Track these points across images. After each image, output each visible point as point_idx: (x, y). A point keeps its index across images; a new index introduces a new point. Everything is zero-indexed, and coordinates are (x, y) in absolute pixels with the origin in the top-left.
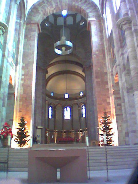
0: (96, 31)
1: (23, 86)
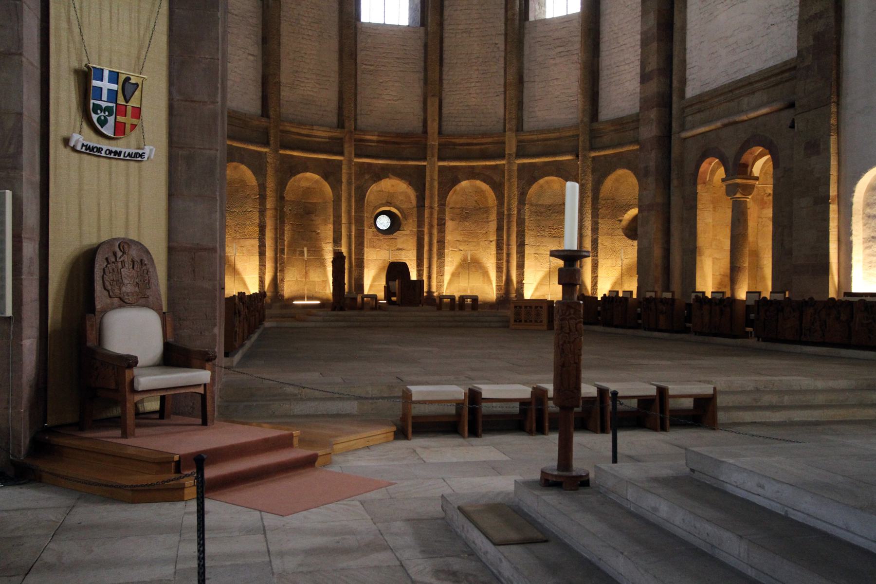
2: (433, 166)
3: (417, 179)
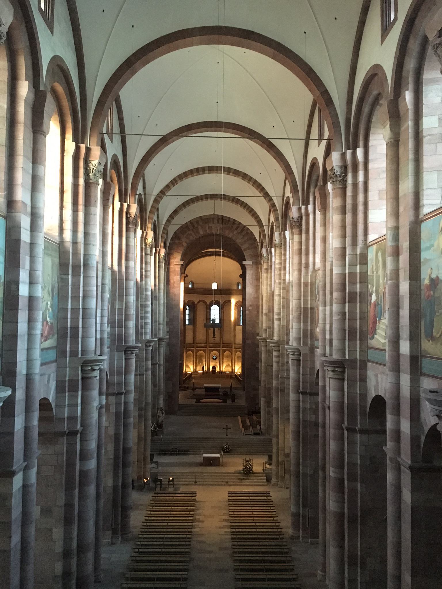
1: (168, 345)
2: (222, 349)
3: (219, 351)
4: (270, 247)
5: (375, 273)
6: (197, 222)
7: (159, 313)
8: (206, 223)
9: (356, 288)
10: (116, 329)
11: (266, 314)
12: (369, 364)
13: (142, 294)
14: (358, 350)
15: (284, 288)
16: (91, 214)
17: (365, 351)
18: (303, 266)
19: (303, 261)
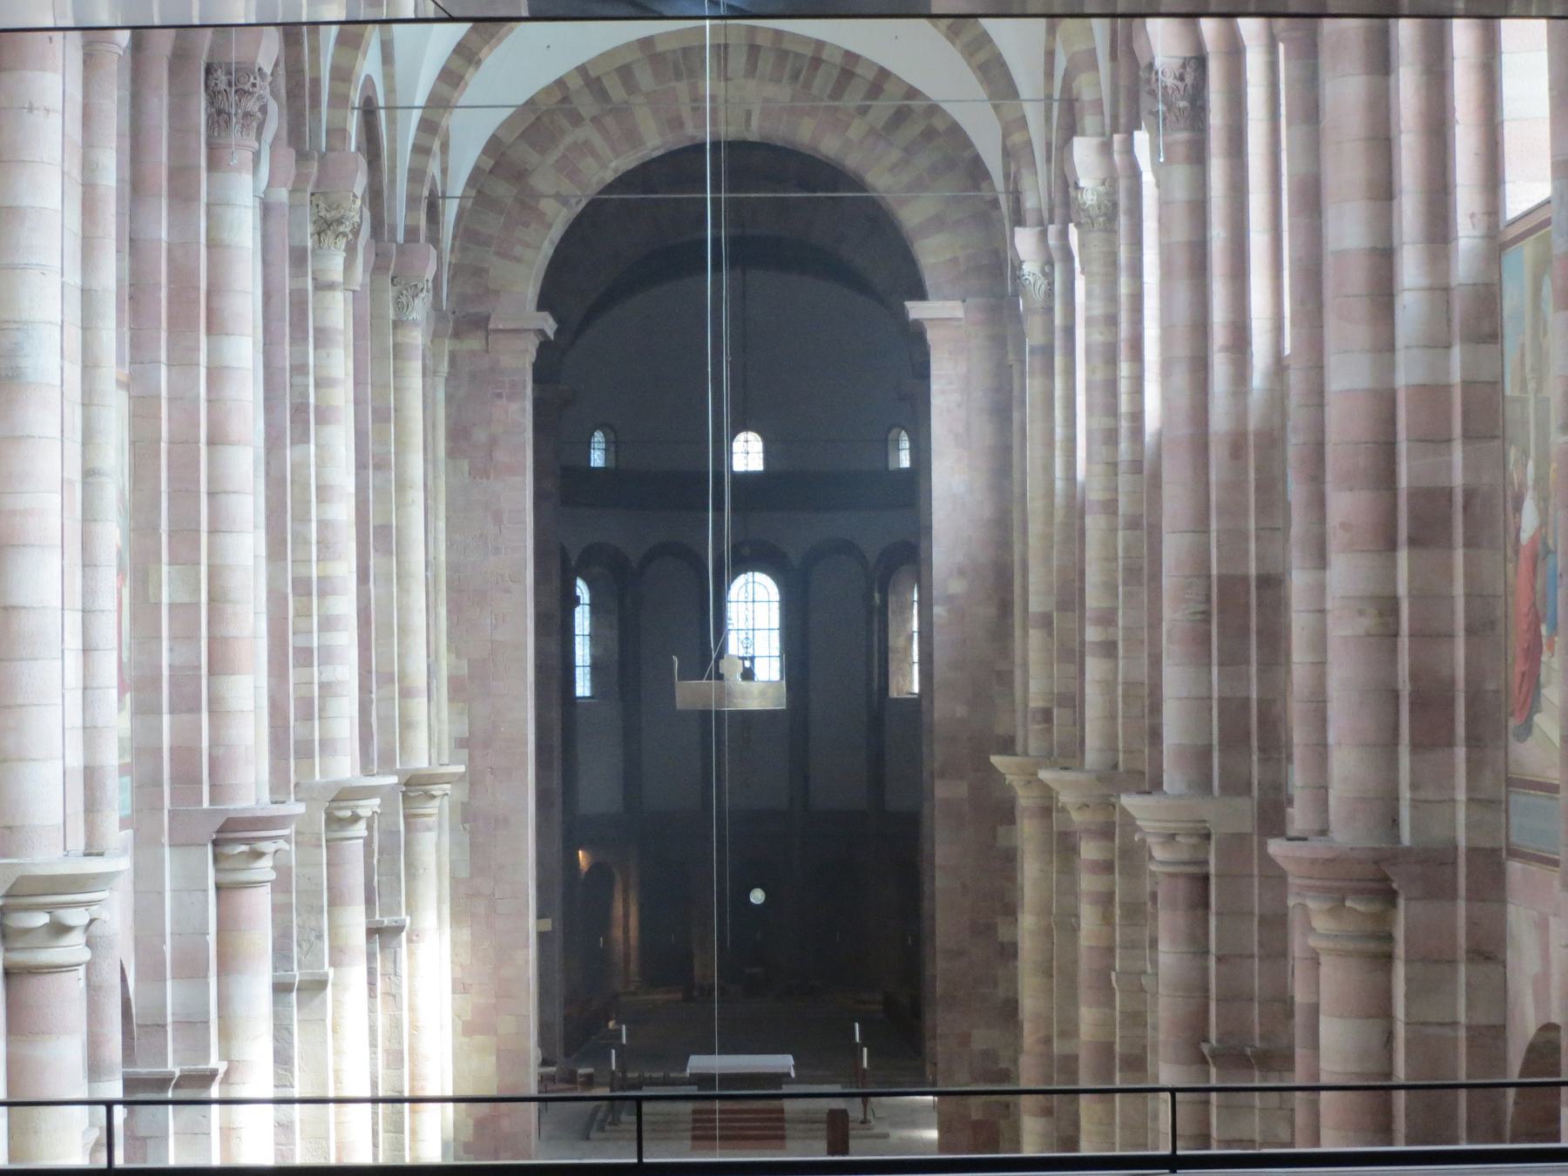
0: (959, 406)
1: (465, 820)
4: (1058, 212)
5: (1531, 385)
6: (625, 73)
7: (404, 630)
8: (678, 76)
9: (1449, 467)
10: (166, 719)
11: (1046, 622)
12: (1515, 868)
13: (302, 518)
14: (1461, 796)
15: (1137, 466)
16: (31, 109)
17: (1491, 803)
18: (1219, 335)
19: (1219, 314)
